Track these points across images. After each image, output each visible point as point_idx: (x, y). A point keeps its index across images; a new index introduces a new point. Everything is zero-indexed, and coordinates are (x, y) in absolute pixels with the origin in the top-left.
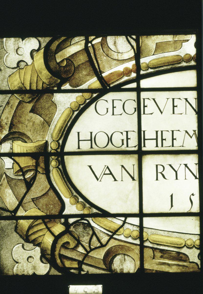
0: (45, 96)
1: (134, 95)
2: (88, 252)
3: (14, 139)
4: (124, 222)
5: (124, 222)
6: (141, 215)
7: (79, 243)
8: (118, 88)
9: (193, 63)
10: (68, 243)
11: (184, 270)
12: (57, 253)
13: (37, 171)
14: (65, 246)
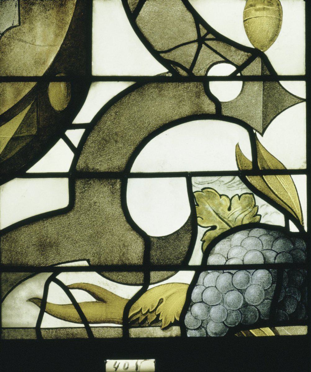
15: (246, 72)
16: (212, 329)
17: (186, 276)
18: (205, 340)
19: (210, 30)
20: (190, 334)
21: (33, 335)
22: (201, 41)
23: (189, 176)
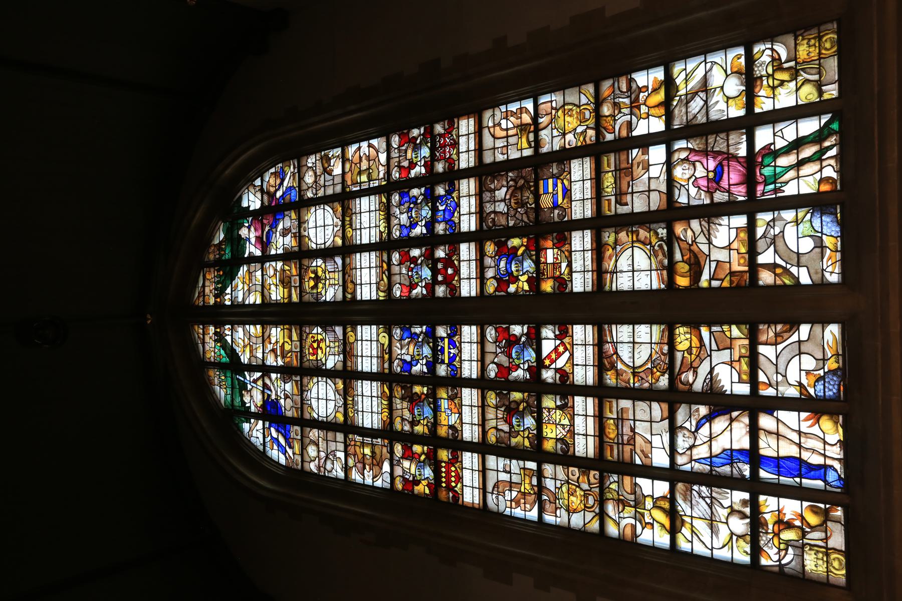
6: (651, 343)
7: (659, 364)
8: (616, 349)
14: (660, 368)
15: (773, 226)
16: (838, 229)
17: (824, 237)
18: (842, 231)
19: (763, 235)
20: (839, 235)
21: (840, 275)
22: (765, 237)
23: (798, 238)
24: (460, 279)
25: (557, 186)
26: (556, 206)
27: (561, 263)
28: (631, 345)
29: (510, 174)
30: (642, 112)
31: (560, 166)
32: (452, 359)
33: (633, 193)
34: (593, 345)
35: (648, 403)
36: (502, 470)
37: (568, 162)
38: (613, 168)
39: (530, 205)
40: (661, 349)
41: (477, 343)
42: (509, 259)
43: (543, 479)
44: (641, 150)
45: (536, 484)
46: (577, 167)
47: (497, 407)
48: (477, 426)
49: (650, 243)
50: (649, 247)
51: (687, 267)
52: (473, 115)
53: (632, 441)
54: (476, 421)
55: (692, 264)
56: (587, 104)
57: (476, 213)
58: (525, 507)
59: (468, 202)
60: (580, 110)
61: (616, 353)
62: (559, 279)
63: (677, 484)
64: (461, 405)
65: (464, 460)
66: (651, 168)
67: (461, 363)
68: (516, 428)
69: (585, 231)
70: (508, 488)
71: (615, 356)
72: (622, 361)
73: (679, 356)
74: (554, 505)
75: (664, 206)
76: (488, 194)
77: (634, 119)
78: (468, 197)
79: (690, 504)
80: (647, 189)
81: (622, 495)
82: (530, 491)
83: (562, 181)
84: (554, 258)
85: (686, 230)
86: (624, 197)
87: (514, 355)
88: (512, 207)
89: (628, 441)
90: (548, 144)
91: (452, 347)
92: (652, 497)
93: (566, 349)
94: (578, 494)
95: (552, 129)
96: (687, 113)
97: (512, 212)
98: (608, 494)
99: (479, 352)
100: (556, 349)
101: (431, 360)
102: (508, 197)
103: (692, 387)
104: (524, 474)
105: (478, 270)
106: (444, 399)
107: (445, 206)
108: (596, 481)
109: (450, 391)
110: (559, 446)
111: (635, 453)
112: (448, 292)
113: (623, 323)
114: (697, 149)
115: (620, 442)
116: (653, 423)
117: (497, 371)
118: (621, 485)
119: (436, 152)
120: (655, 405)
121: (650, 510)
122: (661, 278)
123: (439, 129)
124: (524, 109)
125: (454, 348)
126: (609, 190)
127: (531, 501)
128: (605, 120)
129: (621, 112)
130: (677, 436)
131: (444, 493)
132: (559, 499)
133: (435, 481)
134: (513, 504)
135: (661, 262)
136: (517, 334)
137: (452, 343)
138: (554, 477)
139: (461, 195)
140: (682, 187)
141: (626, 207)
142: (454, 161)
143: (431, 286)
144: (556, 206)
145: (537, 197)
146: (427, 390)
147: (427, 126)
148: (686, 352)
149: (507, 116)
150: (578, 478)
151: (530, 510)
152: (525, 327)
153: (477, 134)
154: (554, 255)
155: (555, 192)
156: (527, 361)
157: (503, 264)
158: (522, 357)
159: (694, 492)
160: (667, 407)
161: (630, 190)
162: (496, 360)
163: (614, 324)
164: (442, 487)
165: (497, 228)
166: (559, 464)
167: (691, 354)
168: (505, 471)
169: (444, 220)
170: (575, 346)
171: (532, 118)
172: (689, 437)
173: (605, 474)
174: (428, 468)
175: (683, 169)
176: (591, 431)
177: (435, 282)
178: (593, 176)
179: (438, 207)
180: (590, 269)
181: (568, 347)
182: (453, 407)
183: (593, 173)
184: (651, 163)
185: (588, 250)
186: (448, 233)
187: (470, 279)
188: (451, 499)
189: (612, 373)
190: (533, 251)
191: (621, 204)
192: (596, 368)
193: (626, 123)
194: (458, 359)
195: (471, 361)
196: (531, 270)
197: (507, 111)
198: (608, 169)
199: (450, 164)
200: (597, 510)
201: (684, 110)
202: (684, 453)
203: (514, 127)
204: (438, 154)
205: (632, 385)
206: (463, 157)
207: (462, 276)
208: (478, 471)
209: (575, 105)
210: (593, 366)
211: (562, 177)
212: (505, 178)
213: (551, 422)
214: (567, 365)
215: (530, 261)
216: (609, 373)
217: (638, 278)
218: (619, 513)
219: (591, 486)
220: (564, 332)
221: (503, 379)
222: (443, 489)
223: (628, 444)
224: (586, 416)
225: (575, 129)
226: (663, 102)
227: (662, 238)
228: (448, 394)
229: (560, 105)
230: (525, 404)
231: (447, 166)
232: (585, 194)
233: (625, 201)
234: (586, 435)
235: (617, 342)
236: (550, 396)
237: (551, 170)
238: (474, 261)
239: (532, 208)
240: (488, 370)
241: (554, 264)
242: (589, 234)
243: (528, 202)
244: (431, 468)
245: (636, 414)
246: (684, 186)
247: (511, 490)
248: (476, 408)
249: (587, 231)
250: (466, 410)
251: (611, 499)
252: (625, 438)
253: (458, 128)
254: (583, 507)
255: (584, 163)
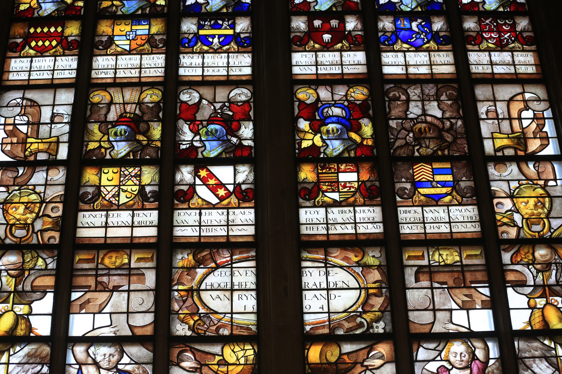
0: (193, 270)
1: (230, 269)
2: (209, 327)
3: (179, 285)
4: (225, 316)
5: (225, 316)
6: (232, 313)
7: (205, 324)
8: (223, 267)
9: (254, 258)
10: (200, 323)
11: (250, 334)
12: (195, 327)
13: (188, 297)
14: (199, 325)
24: (316, 51)
25: (443, 186)
26: (417, 185)
27: (339, 192)
28: (229, 287)
29: (460, 123)
30: (537, 300)
31: (469, 191)
32: (205, 40)
33: (432, 288)
34: (228, 236)
35: (153, 309)
36: (55, 111)
37: (475, 202)
38: (465, 262)
39: (418, 150)
40: (224, 326)
41: (228, 76)
42: (343, 121)
43: (45, 168)
44: (488, 299)
45: (38, 158)
46: (468, 214)
47: (140, 103)
48: (113, 76)
49: (365, 312)
50: (360, 309)
51: (333, 359)
52: (540, 71)
53: (101, 288)
54: (120, 74)
55: (337, 366)
56: (550, 227)
57: (407, 74)
58: (7, 144)
59: (422, 63)
60: (542, 218)
61: (218, 267)
62: (316, 189)
63: (49, 346)
64: (141, 53)
65: (67, 58)
66: (465, 312)
67: (199, 53)
68: (112, 131)
69: (381, 225)
70: (31, 120)
71: (213, 265)
72: (207, 275)
73: (216, 349)
74: (12, 183)
75: (414, 329)
76: (433, 92)
77: (529, 290)
78: (429, 63)
79: (23, 361)
80: (437, 307)
81: (29, 275)
82: (29, 150)
83: (450, 194)
84: (345, 182)
85: (382, 357)
86: (426, 276)
87: (212, 127)
88: (415, 124)
89: (101, 283)
90: (499, 174)
91: (221, 39)
92: (30, 314)
93: (221, 199)
94: (28, 215)
95: (519, 180)
96: (534, 357)
97: (407, 125)
98: (30, 255)
99: (215, 79)
100: (221, 185)
101: (203, 10)
102: (429, 119)
103: (175, 365)
104: (51, 143)
105: (328, 77)
106: (149, 29)
107: (417, 30)
108: (46, 239)
109: (160, 37)
110: (90, 190)
111: (86, 292)
112: (298, 34)
113: (258, 276)
114: (487, 371)
115: (100, 272)
116: (126, 315)
117: (190, 103)
118: (43, 273)
119: (490, 20)
120: (149, 318)
121: (12, 310)
122: (317, 326)
123: (523, 24)
124: (546, 143)
125: (219, 42)
126: (436, 257)
127: (15, 152)
128: (528, 252)
129: (538, 273)
130: (110, 347)
131: (21, 31)
132: (19, 190)
133: (37, 17)
134: (11, 128)
135: (340, 326)
136: (241, 132)
137: (227, 40)
138: (49, 183)
139: (432, 53)
140: (438, 352)
141: (413, 280)
142: (479, 45)
143: (306, 9)
144: (417, 185)
145: (428, 159)
146: (160, 5)
147: (526, 7)
148: (221, 358)
149: (538, 119)
150: (49, 216)
151: (3, 151)
152: (250, 143)
153: (515, 77)
154: (349, 182)
155: (434, 184)
156: (205, 146)
157: (337, 111)
158: (210, 138)
159: (39, 367)
160: (149, 334)
161: (436, 285)
162: (204, 102)
163: (257, 263)
164: (30, 28)
165: (387, 103)
166: (66, 190)
167: (219, 364)
168: (53, 116)
169: (398, 29)
170: (226, 211)
171: (534, 152)
172: (109, 361)
173: (56, 252)
174: (54, 8)
175: (461, 354)
176: (112, 233)
177: (312, 15)
178: (455, 236)
179: (416, 21)
180: (331, 232)
181: (225, 202)
182: (139, 42)
183: (459, 236)
184: (471, 312)
185: (356, 229)
186: (380, 34)
187: (317, 65)
188: (14, 40)
189: (190, 261)
190: (355, 153)
191: (417, 274)
192: (197, 240)
193: (524, 279)
194: (206, 48)
195: (203, 67)
196: (328, 151)
197: (544, 119)
198: (464, 255)
199: (474, 39)
200: (8, 241)
201: (537, 353)
202: (89, 355)
203: (523, 129)
204: (487, 22)
205: (176, 288)
206: (484, 57)
207: (320, 54)
208: (53, 79)
209: (550, 211)
210: (200, 236)
211: (454, 193)
212: (454, 115)
213: (122, 179)
214: (200, 200)
215: (341, 149)
216: (191, 257)
217: (319, 296)
218: (6, 271)
219: (39, 233)
220: (245, 196)
221: (178, 112)
222: (26, 30)
223: (97, 283)
224: (132, 227)
225: (518, 212)
226: (549, 326)
227: (372, 327)
228: (157, 34)
229: (550, 192)
230: (145, 143)
231: (471, 34)
232: (432, 225)
233: (421, 278)
234: (106, 226)
235: (232, 268)
236: (157, 177)
237: (464, 179)
238: (340, 72)
239: (414, 152)
240: (190, 91)
241: (338, 182)
242: (377, 231)
243: (421, 147)
244: (54, 12)
245: (137, 293)
246: (440, 355)
247: (28, 123)
248: (137, 75)
249: (382, 227)
250: (135, 60)
251: (24, 260)
252: (105, 279)
253: (523, 51)
254: (11, 222)
255: (473, 224)
